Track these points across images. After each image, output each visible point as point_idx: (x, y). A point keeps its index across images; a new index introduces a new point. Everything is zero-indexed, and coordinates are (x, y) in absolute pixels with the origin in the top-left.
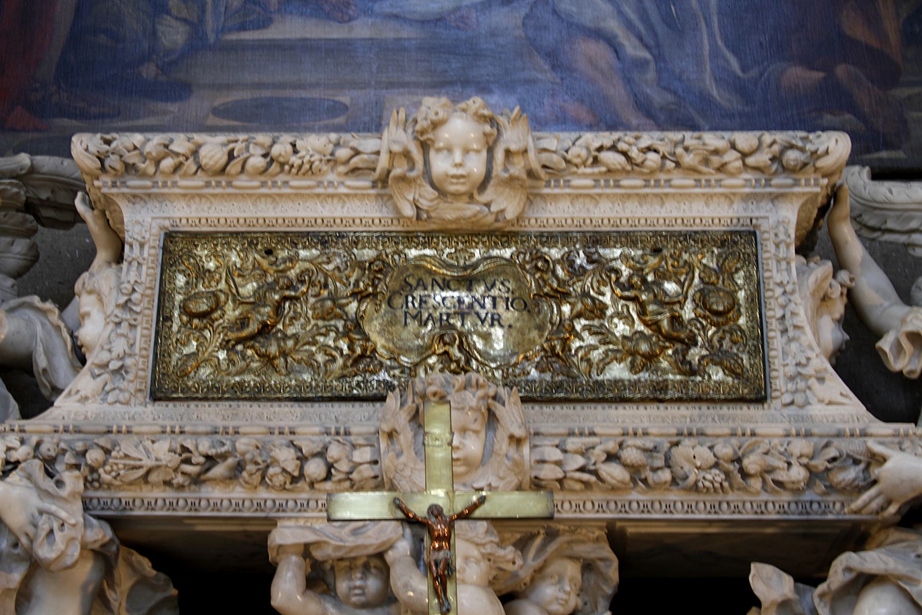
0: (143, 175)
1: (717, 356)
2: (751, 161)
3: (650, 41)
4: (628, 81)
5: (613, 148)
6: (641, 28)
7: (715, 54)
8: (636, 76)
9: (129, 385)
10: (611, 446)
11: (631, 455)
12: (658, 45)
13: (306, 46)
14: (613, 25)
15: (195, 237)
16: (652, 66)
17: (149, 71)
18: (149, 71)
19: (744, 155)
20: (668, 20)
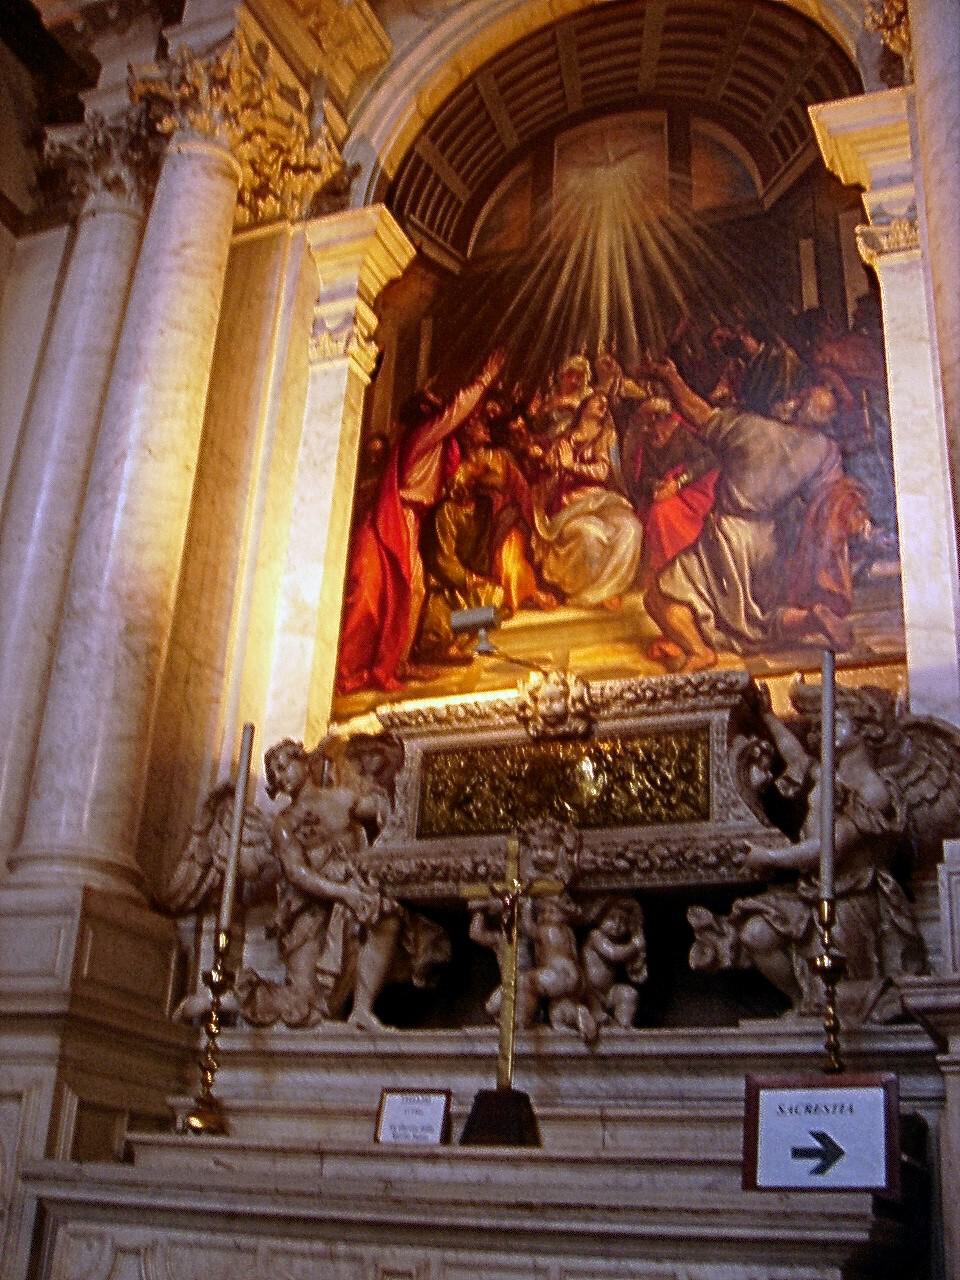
0: (410, 725)
1: (685, 798)
2: (701, 689)
3: (712, 604)
4: (700, 631)
5: (629, 689)
6: (707, 596)
7: (747, 605)
8: (704, 625)
9: (404, 832)
10: (620, 849)
11: (630, 855)
12: (716, 606)
13: (529, 629)
14: (693, 597)
15: (437, 753)
16: (712, 621)
17: (453, 651)
18: (453, 651)
19: (696, 687)
20: (723, 591)
